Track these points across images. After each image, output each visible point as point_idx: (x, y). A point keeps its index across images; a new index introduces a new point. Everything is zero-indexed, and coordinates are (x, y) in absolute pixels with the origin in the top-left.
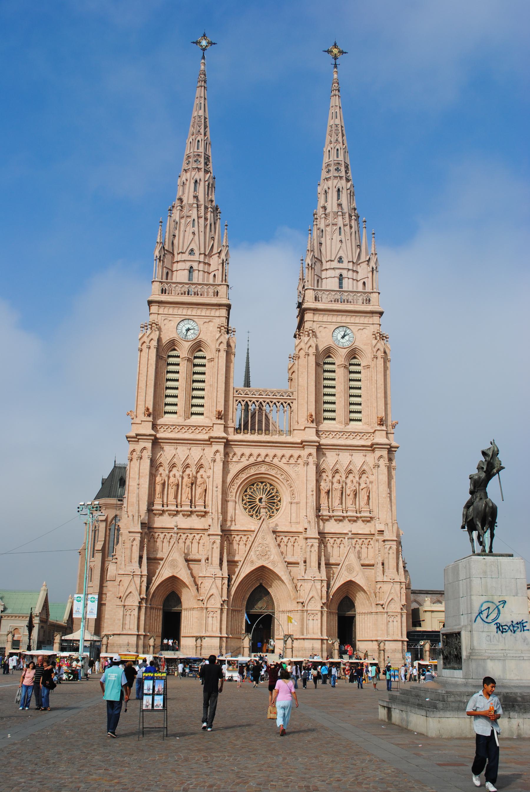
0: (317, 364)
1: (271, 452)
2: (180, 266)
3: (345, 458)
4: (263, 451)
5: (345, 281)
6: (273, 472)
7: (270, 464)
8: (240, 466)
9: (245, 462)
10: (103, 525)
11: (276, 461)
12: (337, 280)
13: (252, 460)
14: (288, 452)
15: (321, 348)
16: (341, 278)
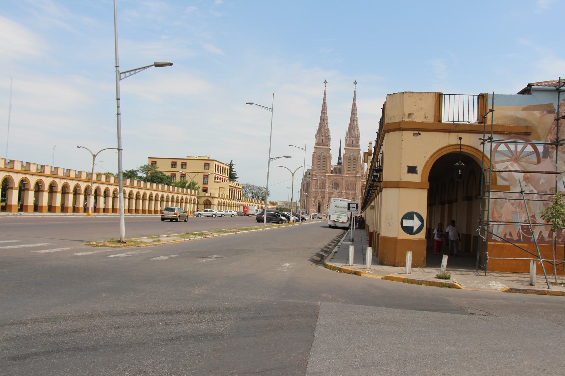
0: (347, 160)
1: (337, 177)
2: (320, 139)
3: (351, 179)
4: (336, 177)
5: (354, 142)
6: (337, 181)
7: (337, 180)
8: (331, 180)
9: (332, 179)
10: (305, 184)
11: (338, 179)
12: (352, 142)
13: (333, 179)
14: (340, 178)
15: (348, 156)
16: (353, 141)
